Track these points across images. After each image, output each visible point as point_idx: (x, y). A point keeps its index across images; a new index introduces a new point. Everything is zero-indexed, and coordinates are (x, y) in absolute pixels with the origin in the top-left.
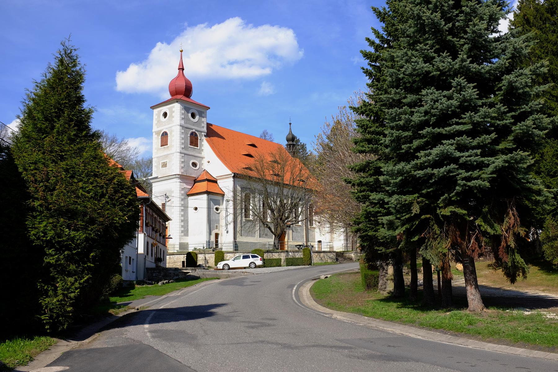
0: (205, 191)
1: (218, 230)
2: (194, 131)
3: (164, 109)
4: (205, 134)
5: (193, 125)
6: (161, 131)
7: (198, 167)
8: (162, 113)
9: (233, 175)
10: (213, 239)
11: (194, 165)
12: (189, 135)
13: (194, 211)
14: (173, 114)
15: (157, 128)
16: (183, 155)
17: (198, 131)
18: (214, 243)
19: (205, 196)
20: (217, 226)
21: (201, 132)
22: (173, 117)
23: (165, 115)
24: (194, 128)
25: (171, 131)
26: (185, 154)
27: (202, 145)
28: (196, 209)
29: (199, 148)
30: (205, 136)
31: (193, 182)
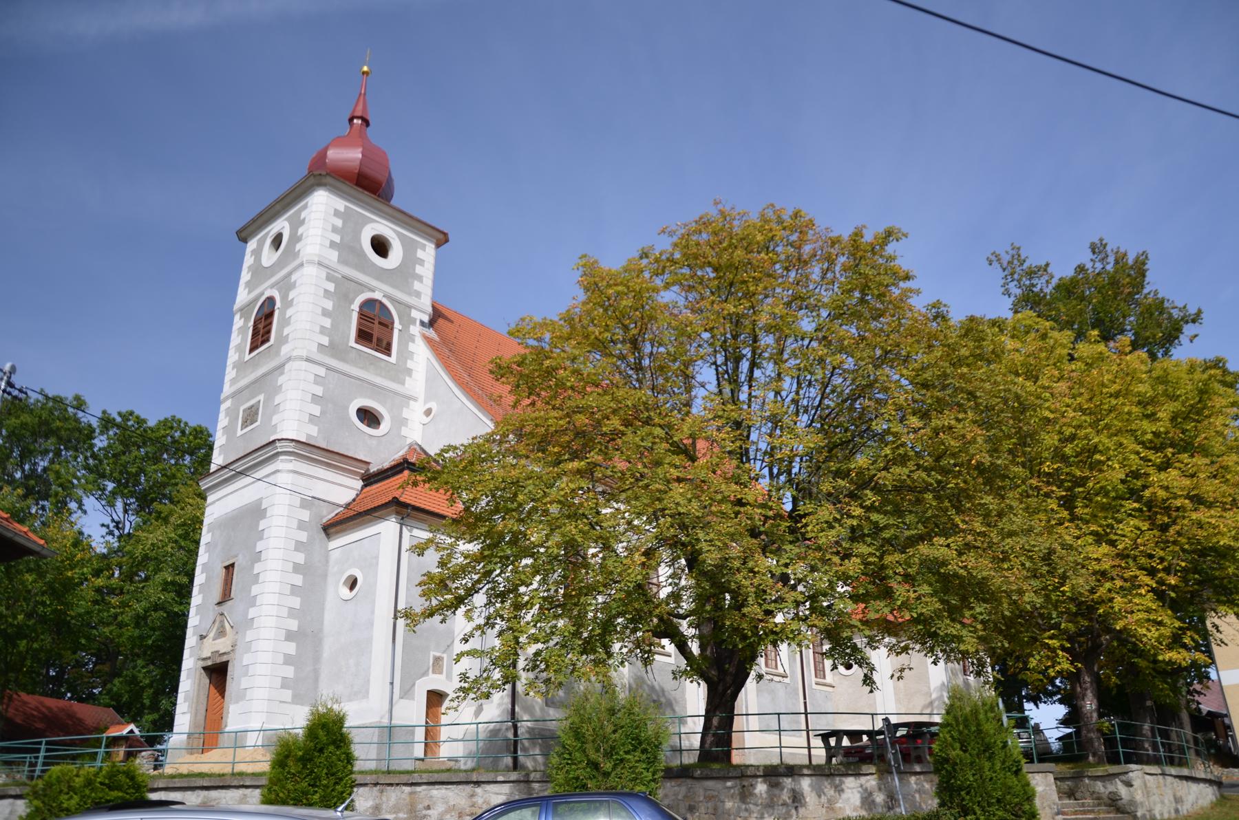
1: (443, 677)
2: (377, 296)
4: (426, 319)
5: (378, 278)
7: (385, 426)
8: (269, 241)
10: (413, 712)
11: (369, 417)
12: (356, 306)
13: (345, 592)
15: (249, 292)
16: (322, 371)
18: (420, 734)
20: (438, 660)
21: (410, 307)
26: (329, 368)
27: (406, 355)
28: (353, 584)
29: (393, 359)
30: (422, 323)
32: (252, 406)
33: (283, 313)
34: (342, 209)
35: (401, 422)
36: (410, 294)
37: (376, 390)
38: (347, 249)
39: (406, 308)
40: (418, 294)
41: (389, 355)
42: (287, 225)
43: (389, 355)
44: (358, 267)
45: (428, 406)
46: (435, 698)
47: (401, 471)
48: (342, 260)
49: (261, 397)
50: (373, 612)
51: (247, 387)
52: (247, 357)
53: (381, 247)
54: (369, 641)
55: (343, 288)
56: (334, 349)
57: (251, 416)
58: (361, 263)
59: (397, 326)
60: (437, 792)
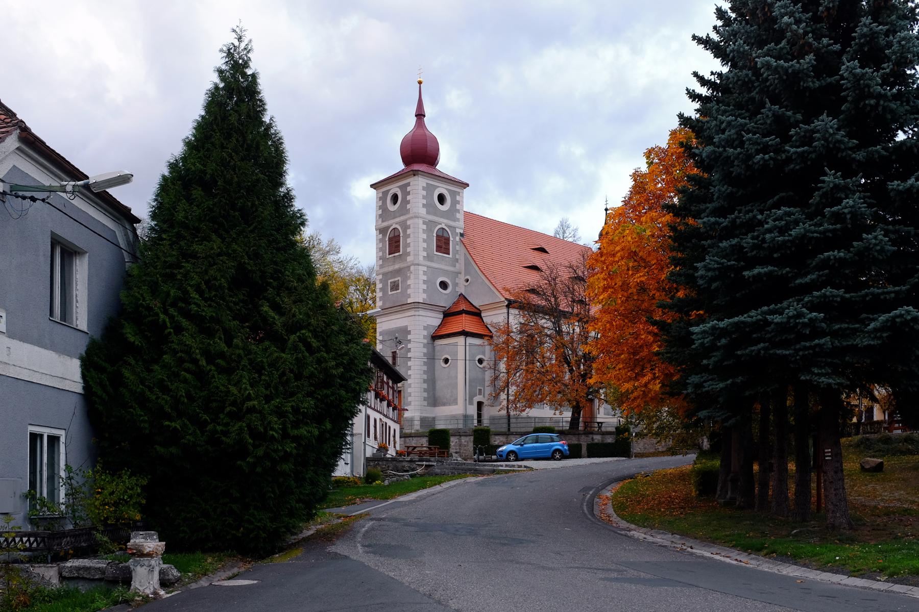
0: (461, 330)
1: (482, 396)
3: (394, 189)
6: (388, 227)
9: (506, 303)
10: (473, 410)
14: (408, 198)
17: (449, 227)
18: (476, 417)
19: (460, 340)
22: (408, 202)
23: (395, 198)
24: (444, 223)
25: (406, 227)
27: (456, 252)
28: (446, 361)
29: (450, 256)
31: (441, 316)
32: (395, 282)
33: (405, 240)
34: (425, 185)
35: (456, 285)
36: (455, 221)
37: (445, 272)
38: (429, 206)
39: (453, 228)
40: (458, 220)
41: (449, 254)
42: (398, 189)
43: (449, 254)
44: (435, 214)
45: (466, 278)
46: (480, 404)
47: (461, 314)
48: (428, 213)
49: (399, 278)
50: (457, 373)
51: (391, 272)
52: (388, 256)
53: (441, 199)
54: (456, 384)
55: (430, 224)
56: (429, 258)
57: (395, 287)
58: (436, 212)
59: (451, 239)
60: (497, 437)
